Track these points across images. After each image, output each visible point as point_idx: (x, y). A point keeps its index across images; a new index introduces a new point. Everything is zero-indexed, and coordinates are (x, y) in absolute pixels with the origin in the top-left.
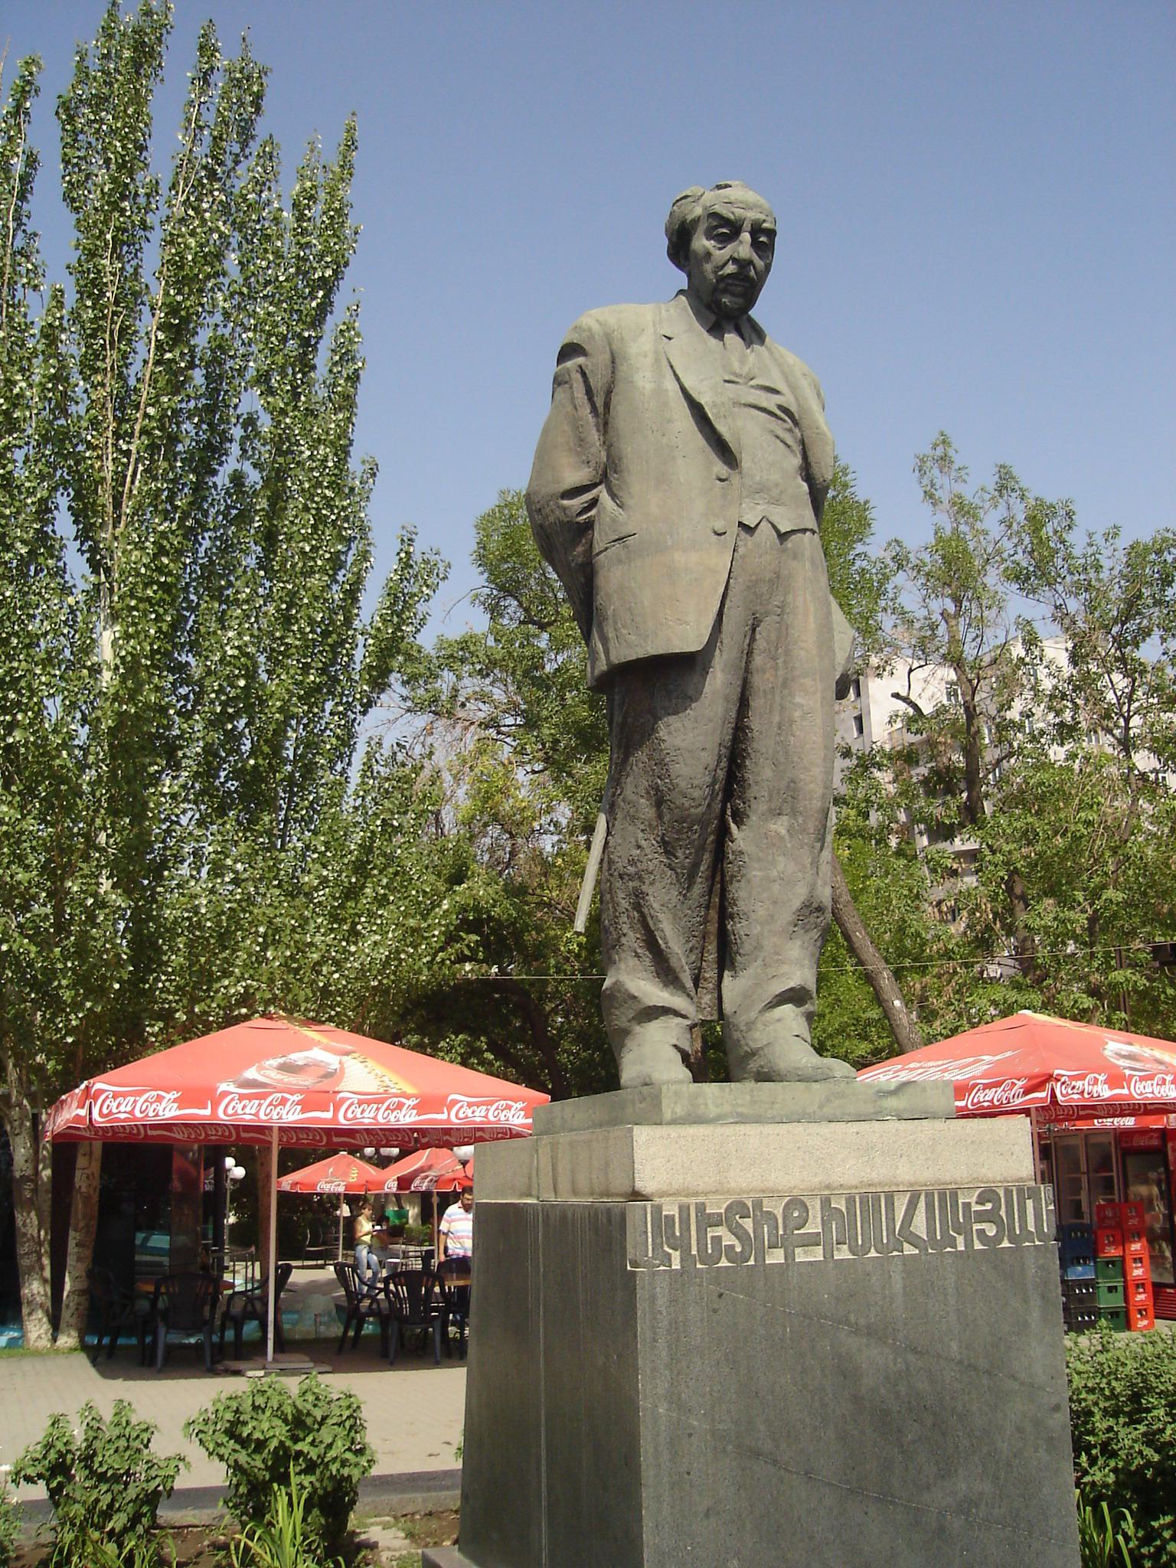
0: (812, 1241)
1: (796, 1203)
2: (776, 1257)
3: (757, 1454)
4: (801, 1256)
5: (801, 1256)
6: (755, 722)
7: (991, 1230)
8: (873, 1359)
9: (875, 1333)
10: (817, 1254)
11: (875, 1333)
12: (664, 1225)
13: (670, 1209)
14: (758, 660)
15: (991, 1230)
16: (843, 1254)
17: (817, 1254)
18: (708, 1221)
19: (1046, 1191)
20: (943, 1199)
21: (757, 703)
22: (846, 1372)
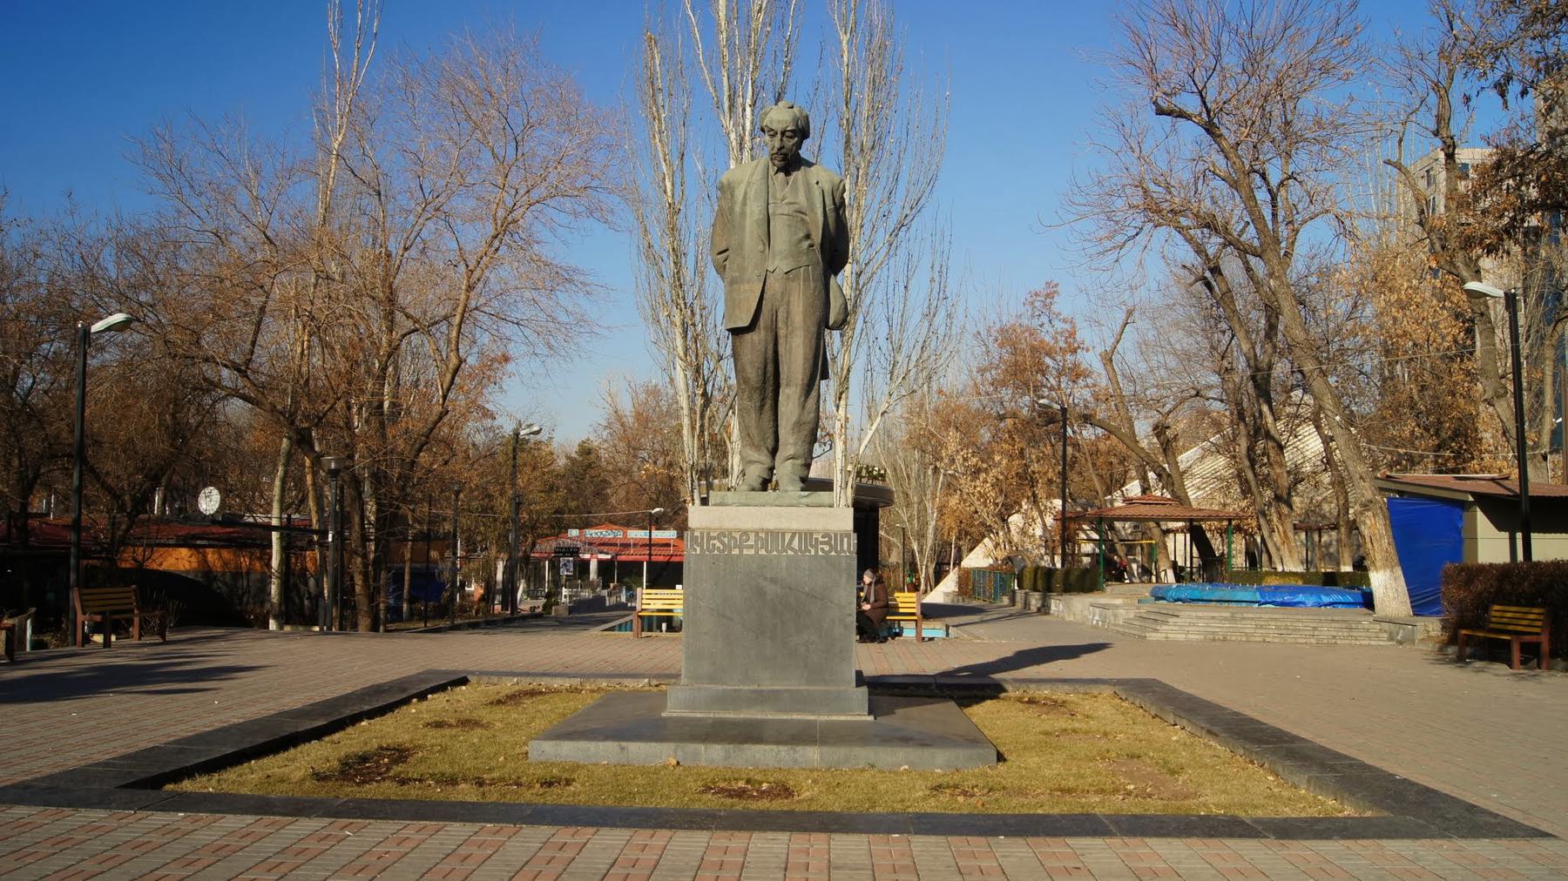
0: (751, 547)
1: (745, 533)
2: (736, 552)
3: (724, 616)
4: (745, 552)
5: (745, 552)
6: (781, 349)
7: (827, 548)
8: (770, 589)
9: (774, 581)
10: (752, 552)
11: (774, 581)
12: (695, 539)
13: (697, 534)
14: (780, 324)
15: (827, 548)
16: (763, 552)
17: (752, 552)
18: (710, 538)
19: (854, 537)
20: (807, 536)
21: (781, 341)
22: (760, 593)
